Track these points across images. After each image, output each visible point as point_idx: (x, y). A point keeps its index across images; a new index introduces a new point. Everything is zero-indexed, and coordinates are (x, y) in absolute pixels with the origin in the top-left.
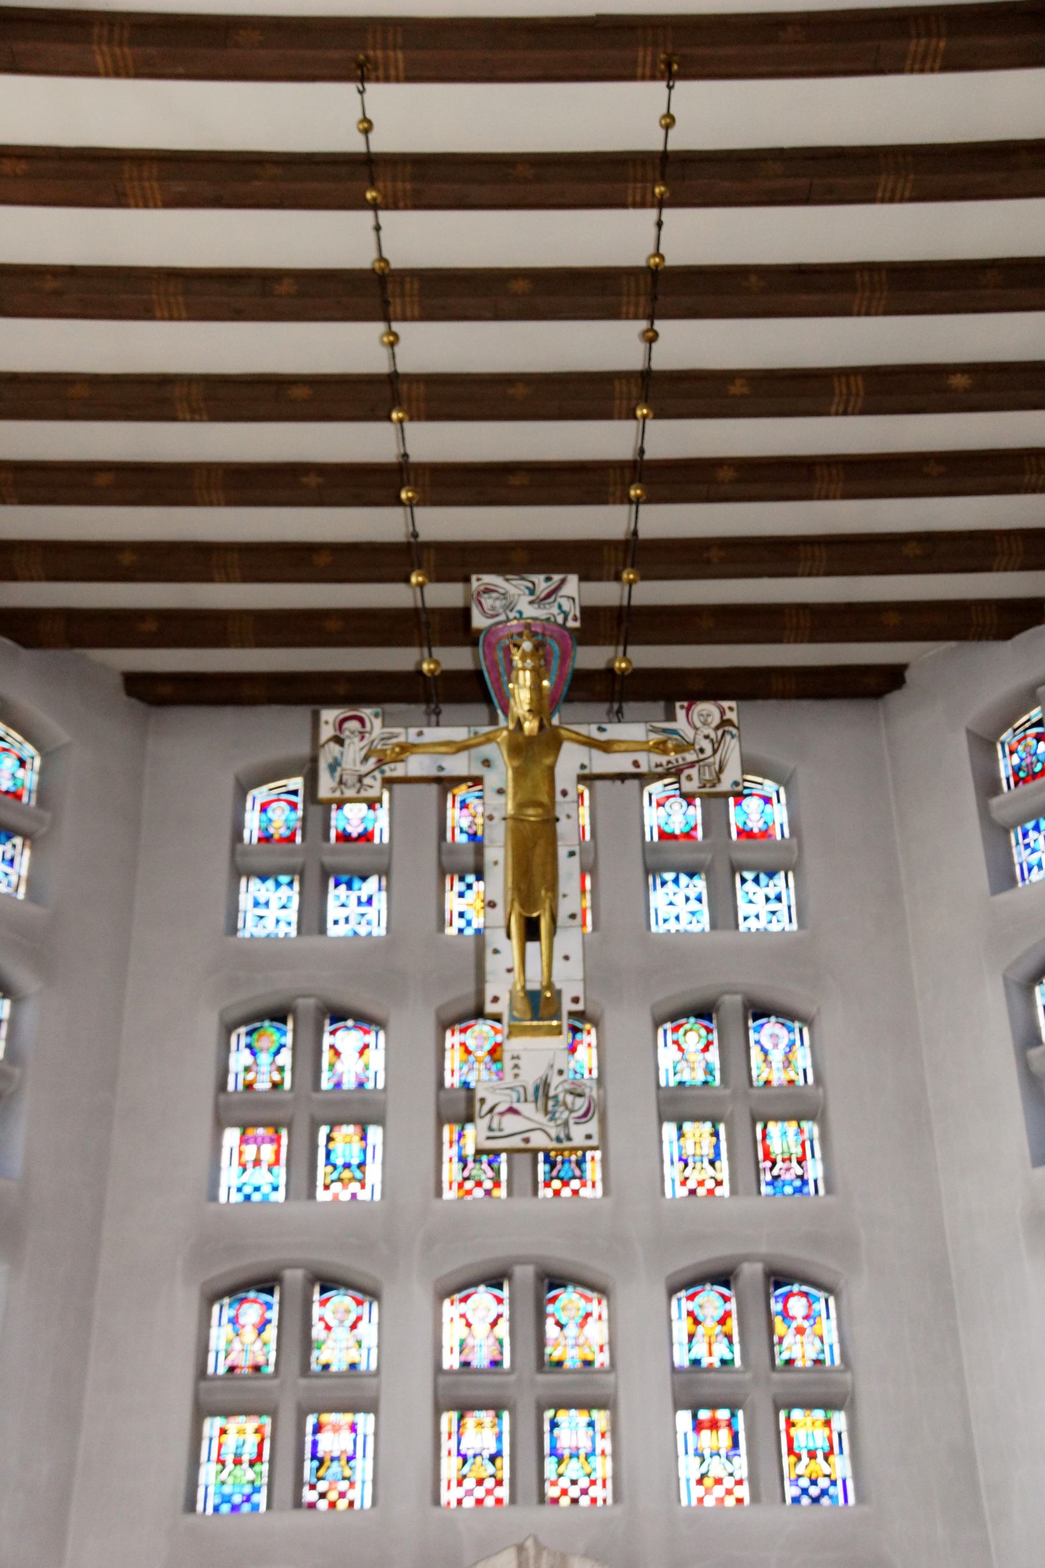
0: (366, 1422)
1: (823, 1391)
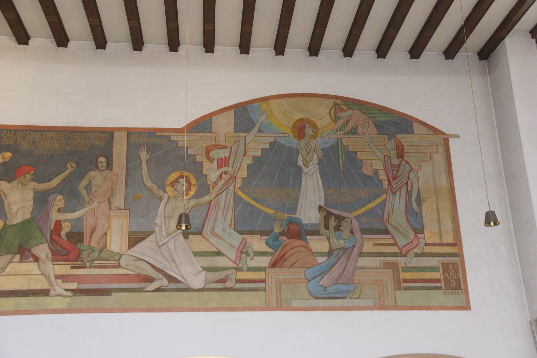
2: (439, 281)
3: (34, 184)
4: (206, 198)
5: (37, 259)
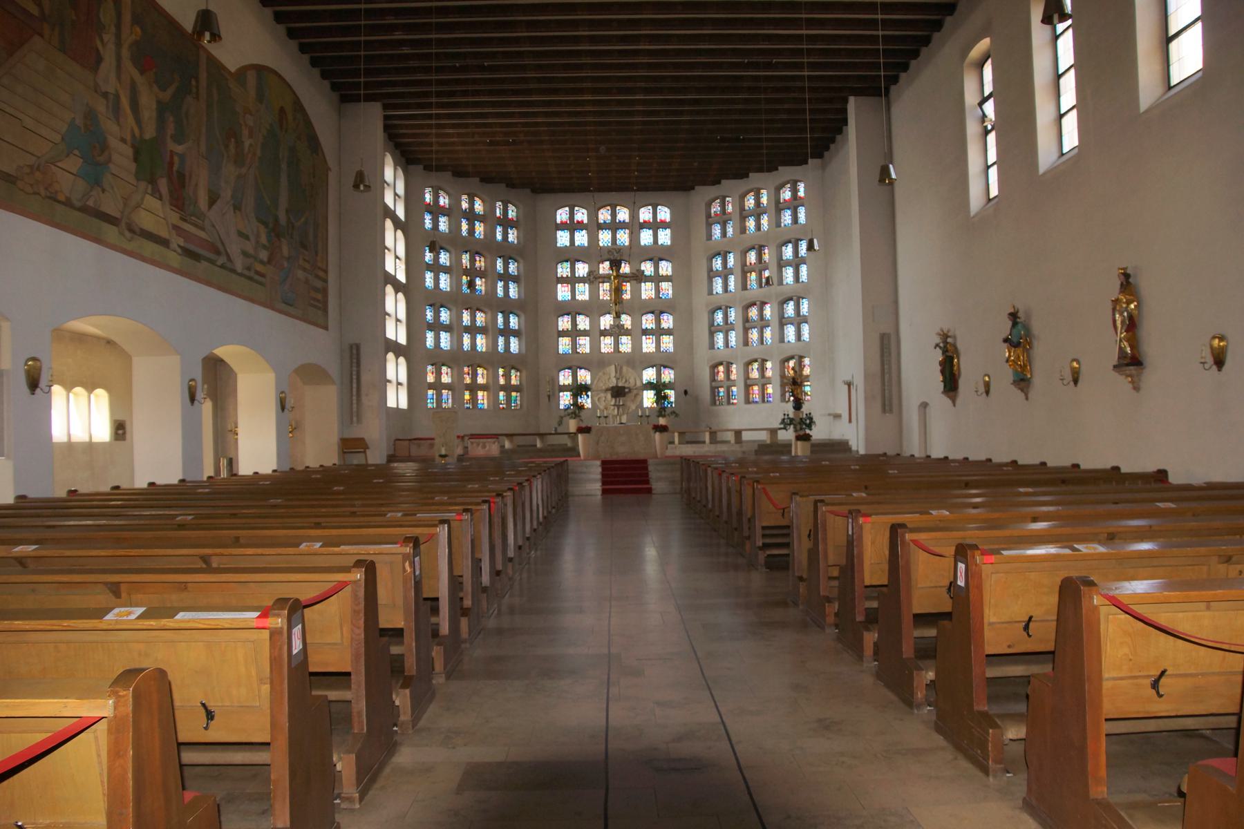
1: (668, 332)
2: (318, 301)
3: (155, 88)
4: (244, 170)
5: (161, 199)
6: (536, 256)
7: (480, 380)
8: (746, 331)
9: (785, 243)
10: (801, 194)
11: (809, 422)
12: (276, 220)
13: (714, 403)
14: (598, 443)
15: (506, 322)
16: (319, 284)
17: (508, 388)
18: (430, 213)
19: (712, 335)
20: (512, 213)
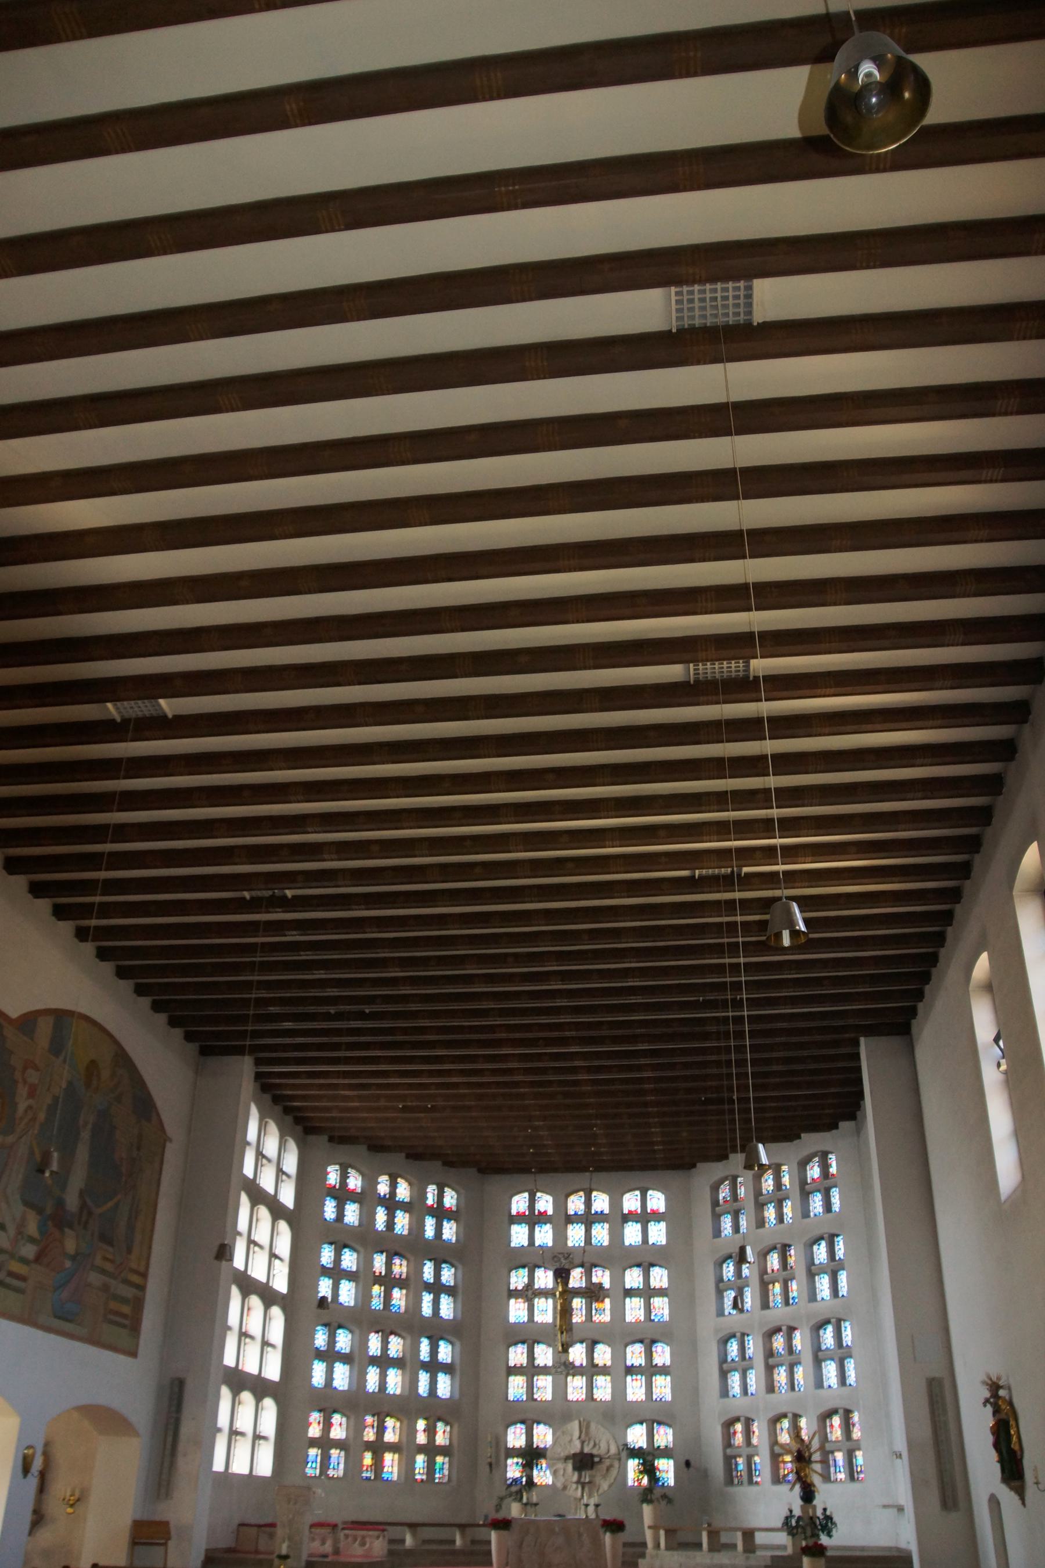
0: (550, 1378)
1: (664, 1371)
2: (124, 1316)
4: (10, 1139)
6: (480, 1257)
7: (390, 1437)
8: (770, 1369)
9: (817, 1240)
10: (833, 1170)
11: (827, 1524)
12: (60, 1204)
13: (730, 1481)
14: (520, 1546)
15: (434, 1351)
16: (129, 1292)
17: (431, 1450)
18: (335, 1198)
19: (724, 1375)
20: (450, 1199)
